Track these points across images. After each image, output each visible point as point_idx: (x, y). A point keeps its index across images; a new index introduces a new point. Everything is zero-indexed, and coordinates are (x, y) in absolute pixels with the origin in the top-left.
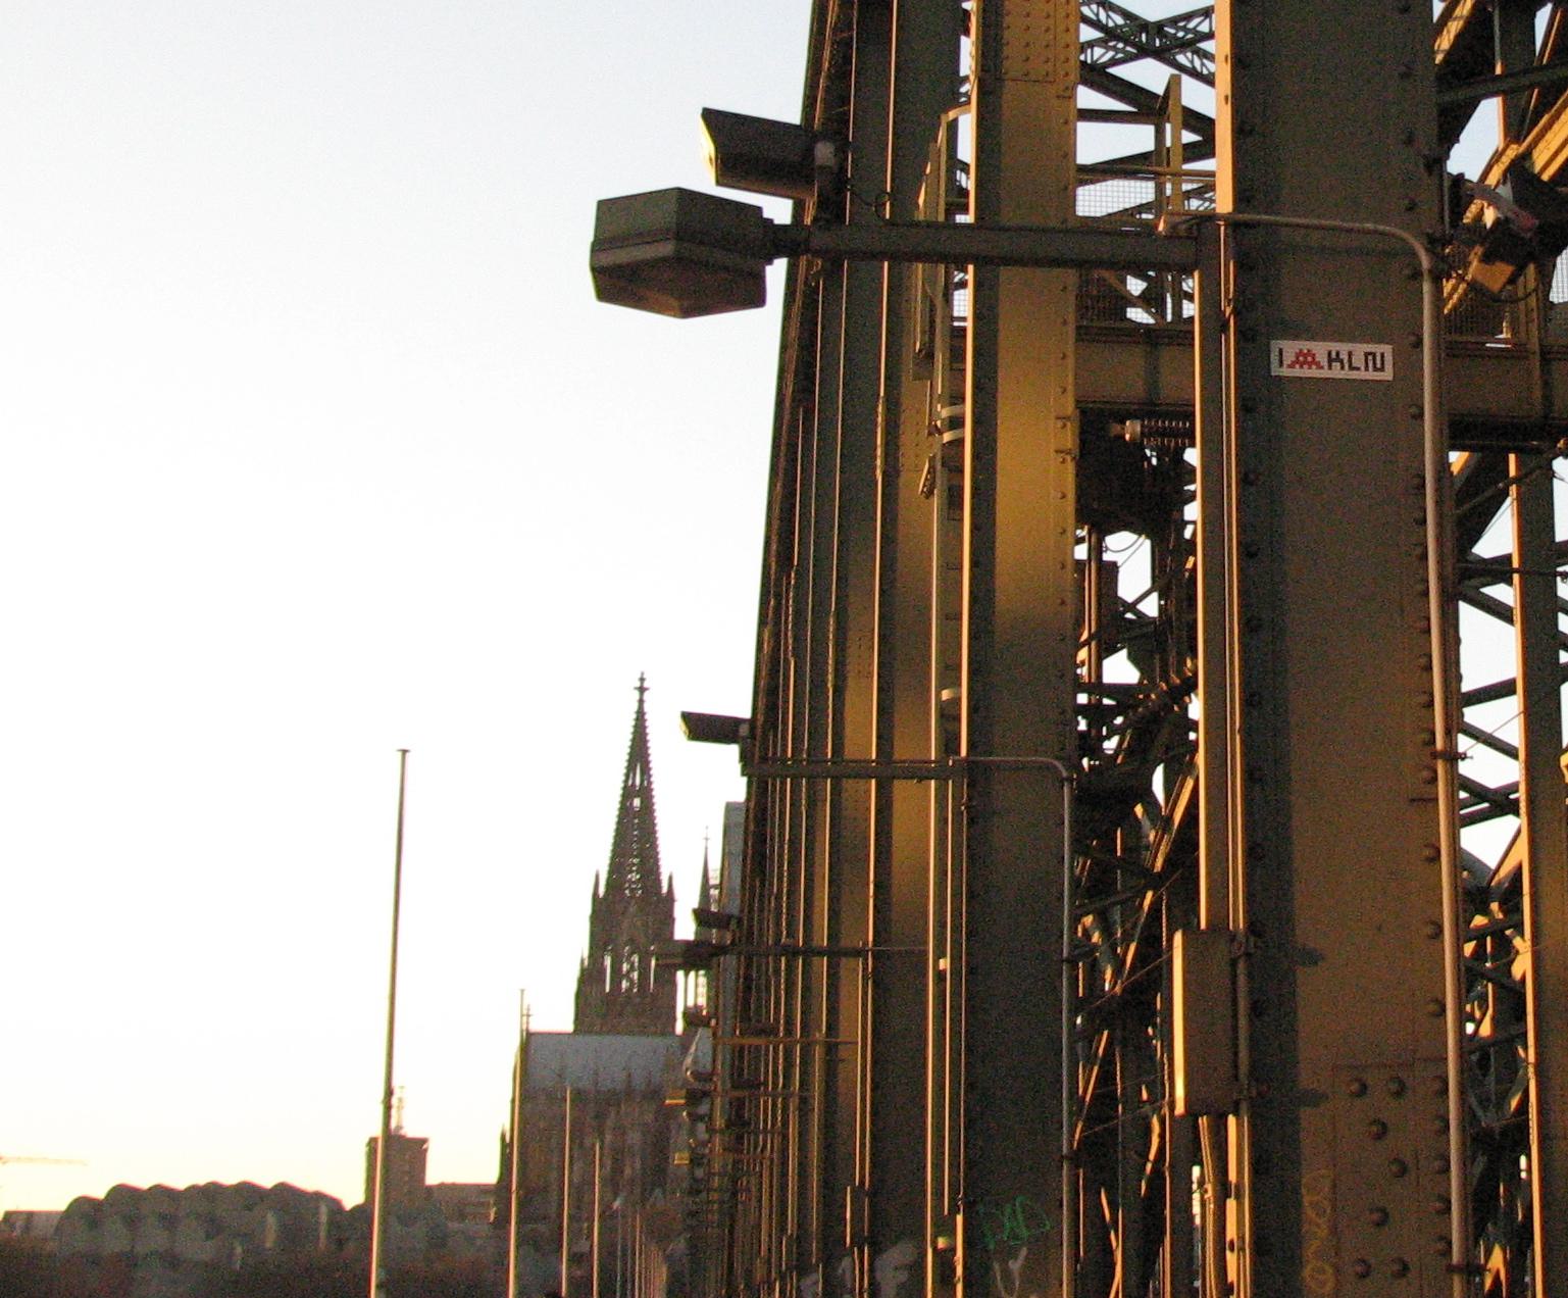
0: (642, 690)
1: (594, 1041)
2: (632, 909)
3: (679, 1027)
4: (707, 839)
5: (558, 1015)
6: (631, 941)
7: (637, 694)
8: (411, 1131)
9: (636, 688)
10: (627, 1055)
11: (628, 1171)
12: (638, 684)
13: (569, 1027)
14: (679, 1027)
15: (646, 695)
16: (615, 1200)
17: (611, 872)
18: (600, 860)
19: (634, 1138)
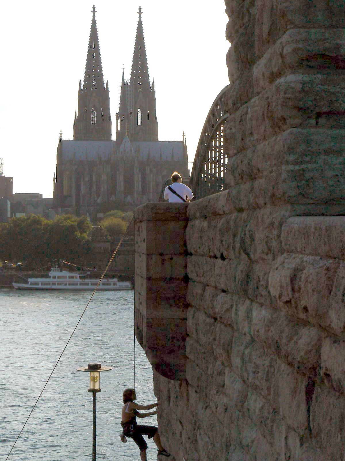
2: (94, 94)
3: (114, 137)
4: (123, 69)
5: (69, 135)
6: (94, 106)
9: (91, 11)
10: (93, 148)
11: (102, 189)
12: (92, 10)
13: (73, 139)
14: (114, 137)
18: (82, 77)
19: (104, 178)
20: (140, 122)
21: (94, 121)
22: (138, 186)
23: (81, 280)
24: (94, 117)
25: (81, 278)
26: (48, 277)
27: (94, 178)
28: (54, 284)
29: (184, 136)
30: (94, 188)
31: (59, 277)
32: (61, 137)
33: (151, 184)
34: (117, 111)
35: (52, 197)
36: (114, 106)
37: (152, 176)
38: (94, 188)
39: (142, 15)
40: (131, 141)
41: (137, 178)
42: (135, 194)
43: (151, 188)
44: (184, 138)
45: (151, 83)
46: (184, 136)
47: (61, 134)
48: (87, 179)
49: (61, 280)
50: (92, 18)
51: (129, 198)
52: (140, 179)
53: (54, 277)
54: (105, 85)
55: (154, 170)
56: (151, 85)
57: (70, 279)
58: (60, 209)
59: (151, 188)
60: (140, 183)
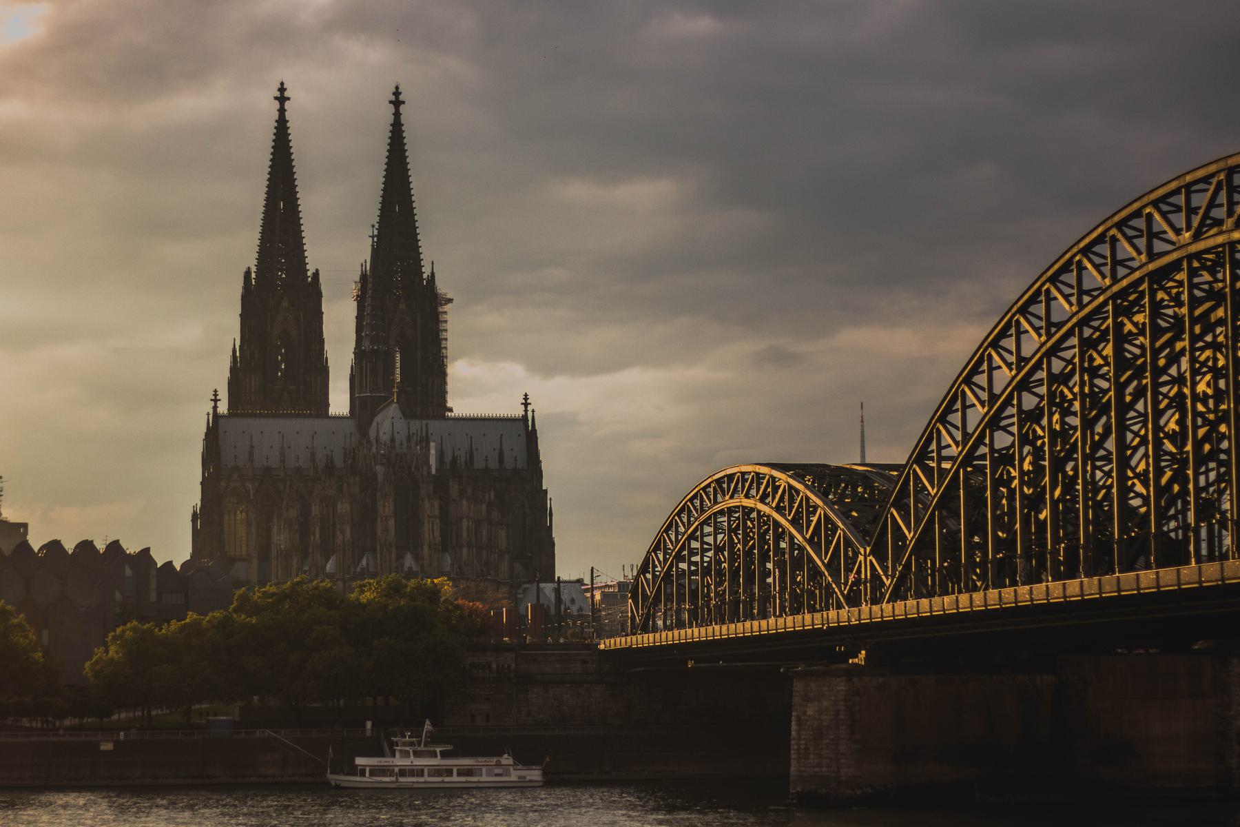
2: (285, 304)
9: (276, 98)
11: (340, 538)
19: (344, 508)
22: (430, 531)
27: (315, 510)
29: (526, 404)
33: (465, 524)
37: (465, 503)
39: (402, 108)
40: (408, 414)
41: (430, 508)
42: (426, 548)
43: (465, 534)
44: (526, 411)
46: (526, 404)
48: (293, 513)
52: (437, 512)
59: (465, 534)
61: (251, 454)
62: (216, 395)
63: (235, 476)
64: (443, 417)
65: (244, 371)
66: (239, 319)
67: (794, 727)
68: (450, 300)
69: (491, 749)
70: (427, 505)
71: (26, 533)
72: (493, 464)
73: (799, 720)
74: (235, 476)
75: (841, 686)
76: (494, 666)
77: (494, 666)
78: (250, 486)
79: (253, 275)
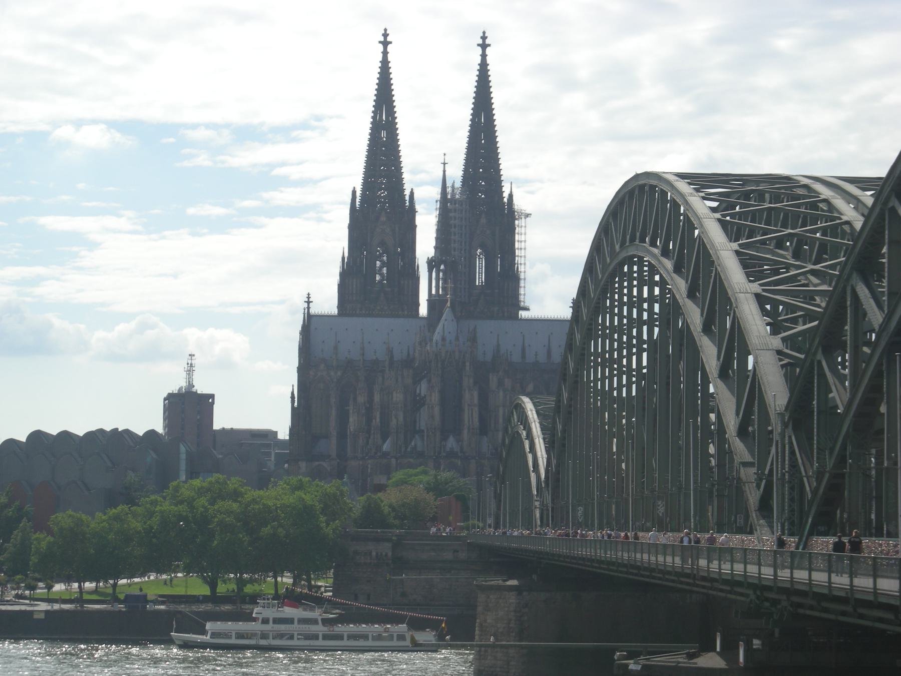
0: (385, 43)
1: (356, 323)
3: (423, 310)
4: (444, 164)
6: (382, 244)
7: (381, 48)
8: (201, 388)
9: (380, 42)
10: (380, 334)
11: (394, 421)
12: (382, 39)
13: (334, 311)
14: (423, 310)
15: (389, 46)
16: (384, 441)
17: (364, 190)
18: (357, 181)
20: (480, 278)
21: (381, 275)
22: (471, 416)
23: (326, 629)
24: (381, 268)
25: (325, 622)
26: (249, 618)
27: (377, 398)
28: (264, 636)
30: (377, 421)
31: (277, 621)
32: (309, 308)
34: (431, 253)
35: (287, 438)
36: (425, 244)
37: (501, 393)
38: (377, 421)
39: (488, 50)
41: (471, 397)
42: (466, 431)
43: (501, 420)
45: (506, 195)
47: (309, 302)
48: (361, 399)
49: (283, 627)
50: (380, 57)
51: (451, 442)
52: (476, 401)
53: (265, 621)
54: (407, 198)
55: (508, 383)
56: (505, 200)
57: (301, 626)
58: (303, 465)
59: (501, 420)
60: (476, 409)
61: (336, 348)
62: (309, 298)
63: (322, 366)
64: (516, 317)
65: (353, 275)
66: (347, 230)
67: (477, 632)
68: (527, 215)
69: (397, 620)
70: (467, 396)
71: (213, 403)
72: (542, 358)
73: (481, 625)
74: (322, 366)
75: (512, 598)
76: (374, 554)
77: (374, 554)
78: (332, 373)
79: (358, 193)
